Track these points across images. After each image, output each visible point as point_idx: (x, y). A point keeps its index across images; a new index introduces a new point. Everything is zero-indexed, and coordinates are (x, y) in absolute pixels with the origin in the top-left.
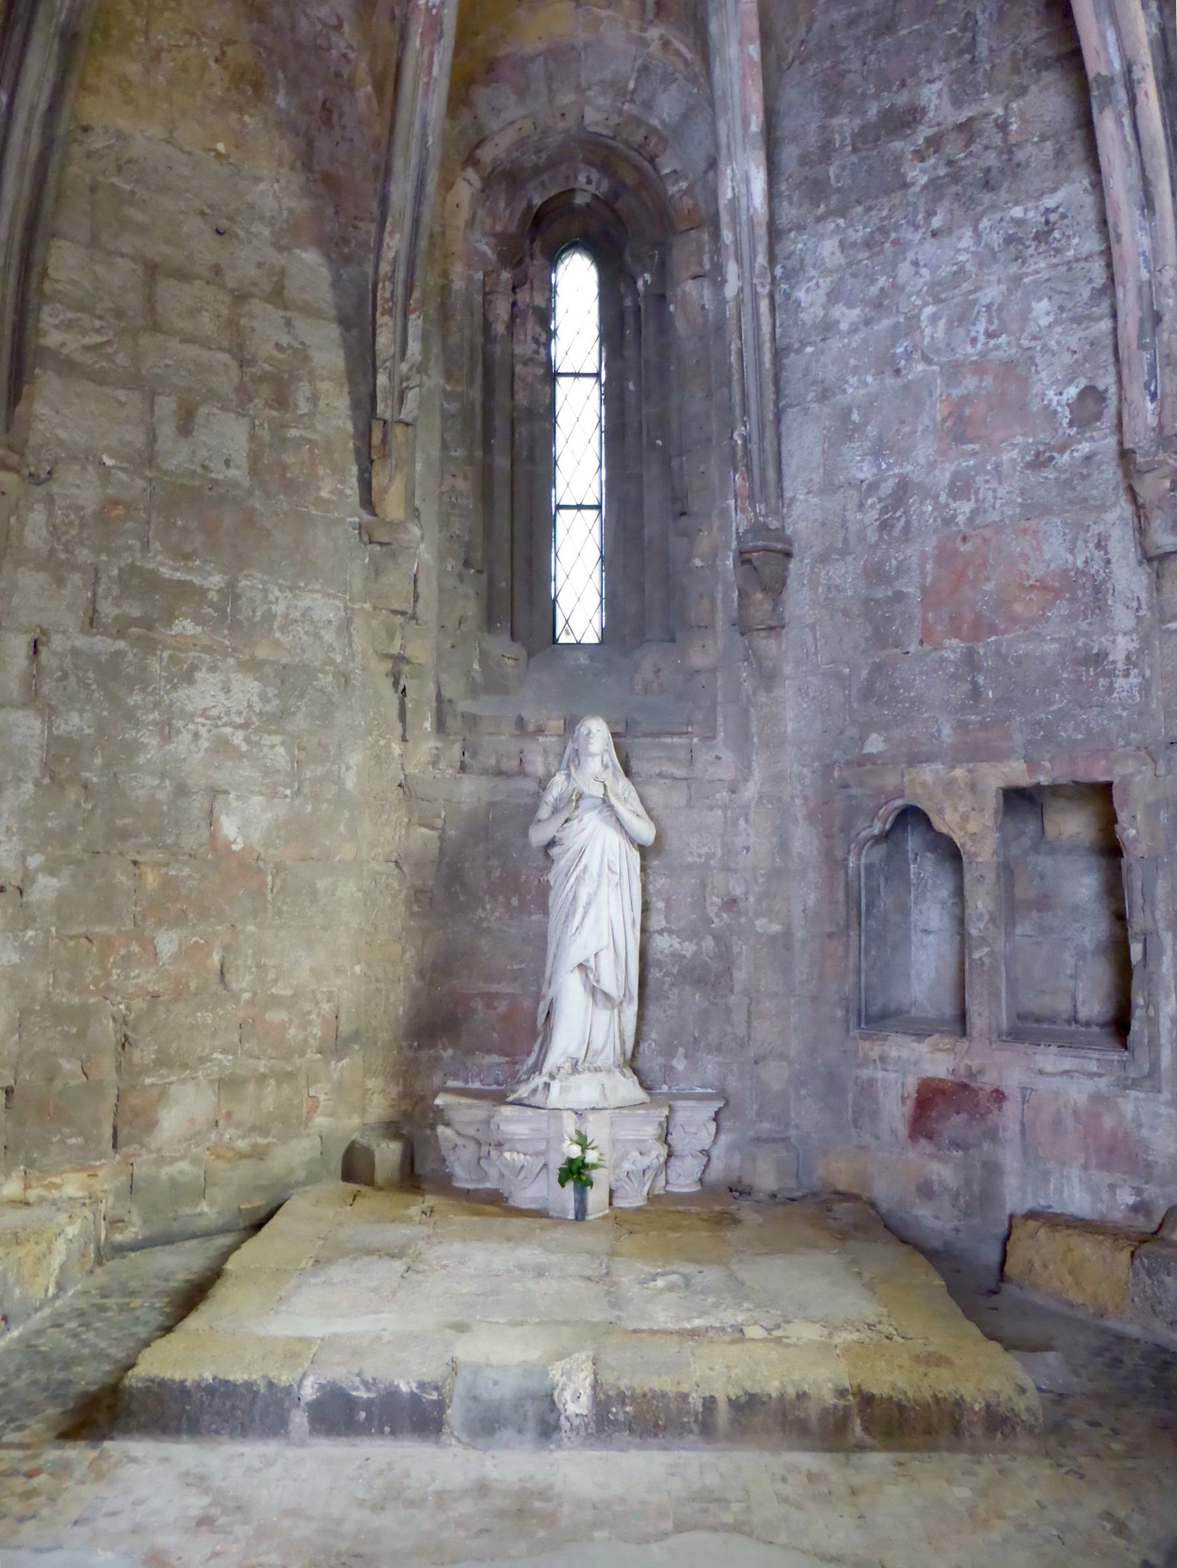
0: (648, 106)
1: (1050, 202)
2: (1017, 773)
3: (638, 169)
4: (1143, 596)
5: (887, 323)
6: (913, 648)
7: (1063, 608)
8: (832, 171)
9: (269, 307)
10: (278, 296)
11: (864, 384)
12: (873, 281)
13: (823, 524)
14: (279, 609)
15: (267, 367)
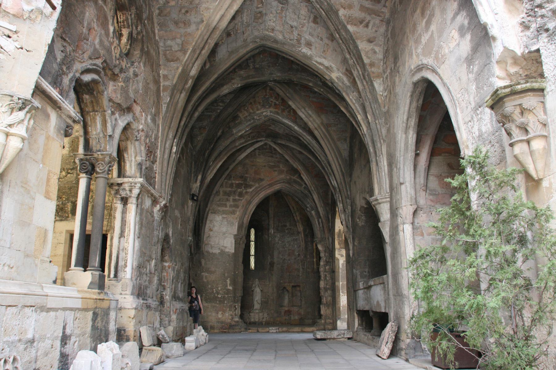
2: (293, 284)
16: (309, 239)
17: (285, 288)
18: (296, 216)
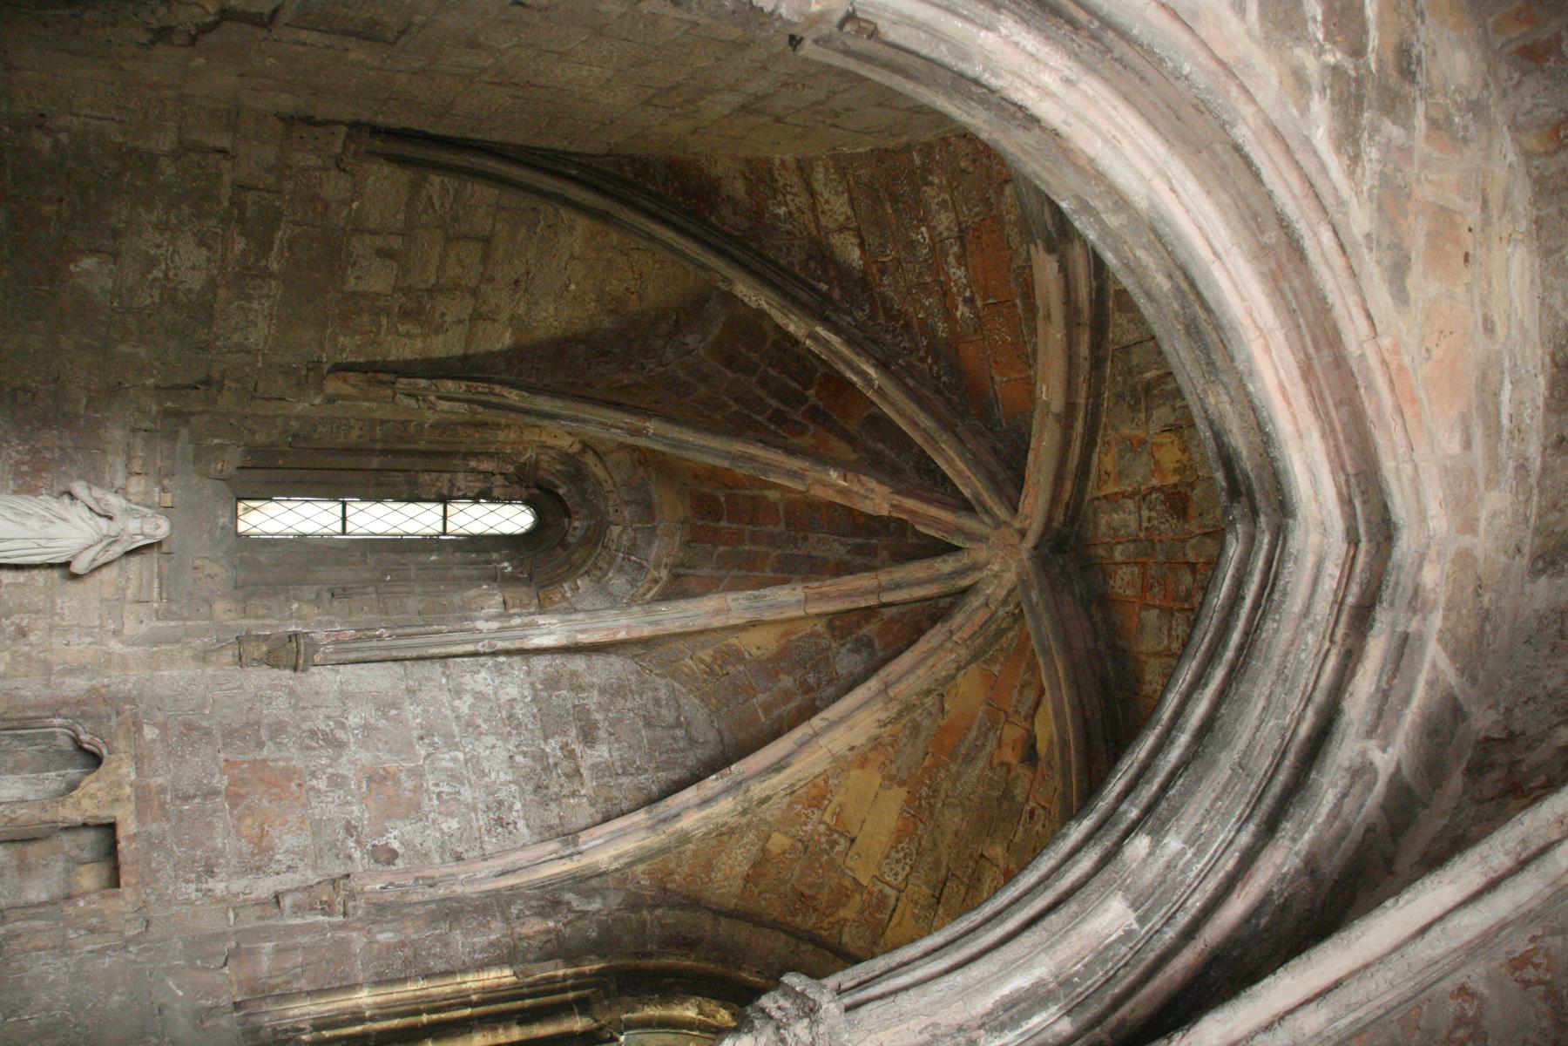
0: (620, 570)
1: (521, 824)
3: (584, 562)
4: (253, 896)
5: (456, 730)
6: (222, 756)
7: (246, 848)
8: (564, 693)
9: (471, 311)
10: (477, 316)
11: (416, 717)
12: (485, 721)
13: (317, 693)
14: (255, 305)
15: (428, 307)
16: (534, 926)
17: (94, 760)
18: (705, 802)
